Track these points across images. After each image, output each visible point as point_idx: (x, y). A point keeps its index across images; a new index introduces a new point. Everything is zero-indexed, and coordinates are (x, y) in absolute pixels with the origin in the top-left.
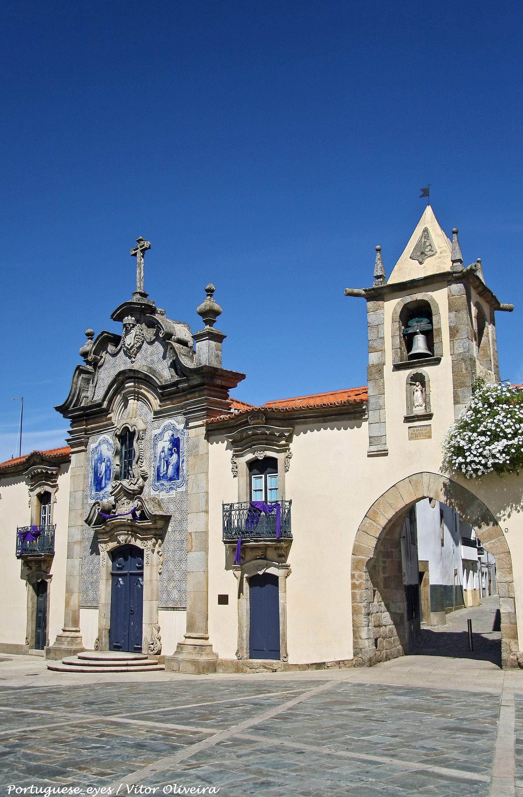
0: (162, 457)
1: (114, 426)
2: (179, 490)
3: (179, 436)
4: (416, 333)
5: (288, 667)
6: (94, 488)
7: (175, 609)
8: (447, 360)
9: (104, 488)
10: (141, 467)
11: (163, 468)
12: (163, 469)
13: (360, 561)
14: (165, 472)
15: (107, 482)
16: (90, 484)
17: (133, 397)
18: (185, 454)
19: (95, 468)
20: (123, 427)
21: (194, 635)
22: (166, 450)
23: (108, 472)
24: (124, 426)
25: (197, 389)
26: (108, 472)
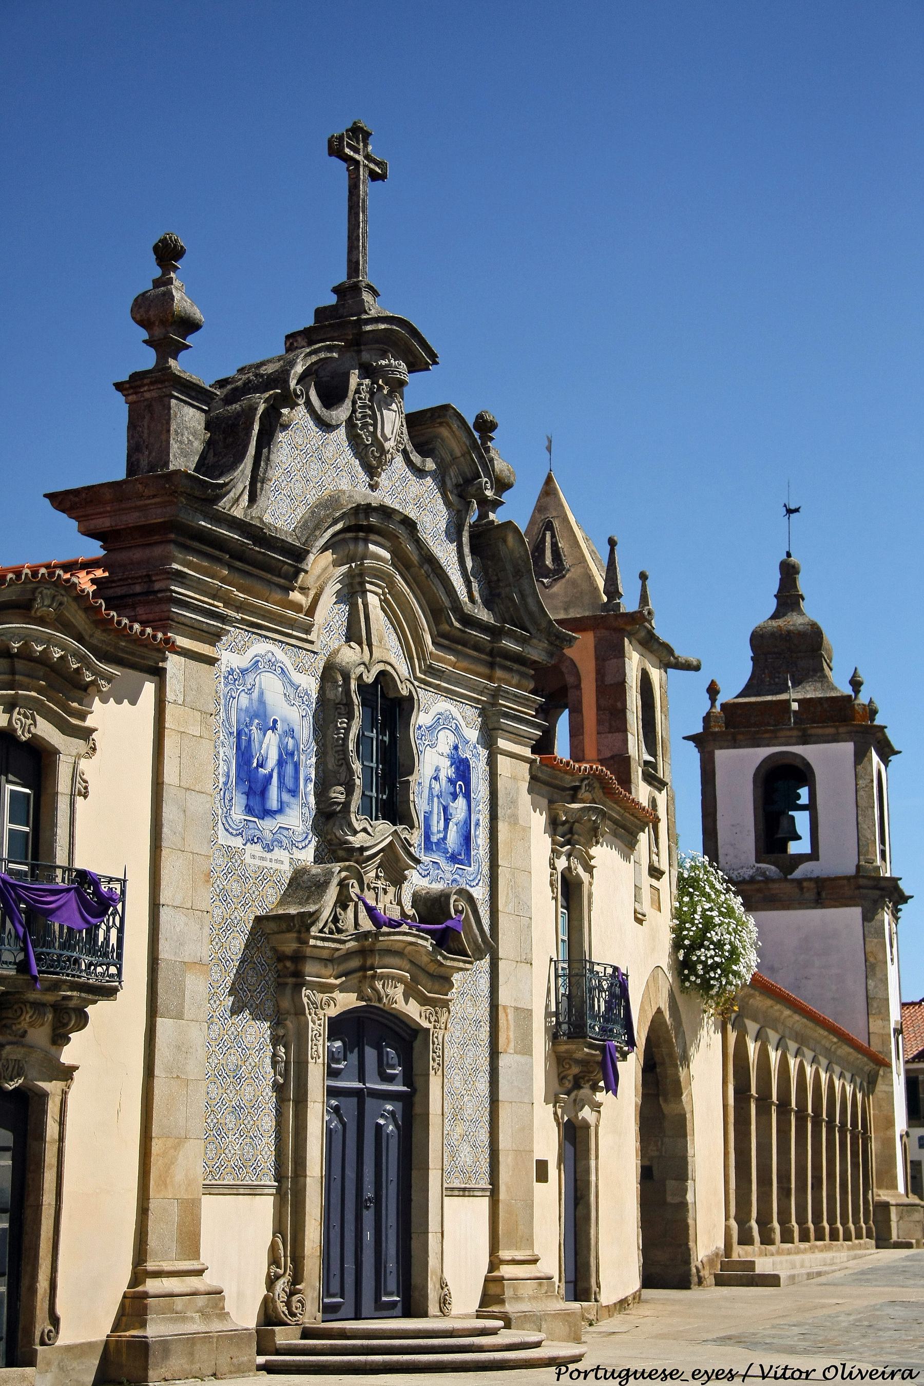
0: (435, 793)
1: (309, 638)
3: (468, 757)
6: (239, 801)
7: (467, 1193)
9: (276, 812)
11: (438, 822)
14: (442, 835)
15: (286, 797)
16: (222, 779)
17: (380, 591)
18: (481, 806)
23: (289, 769)
25: (516, 667)
26: (289, 769)
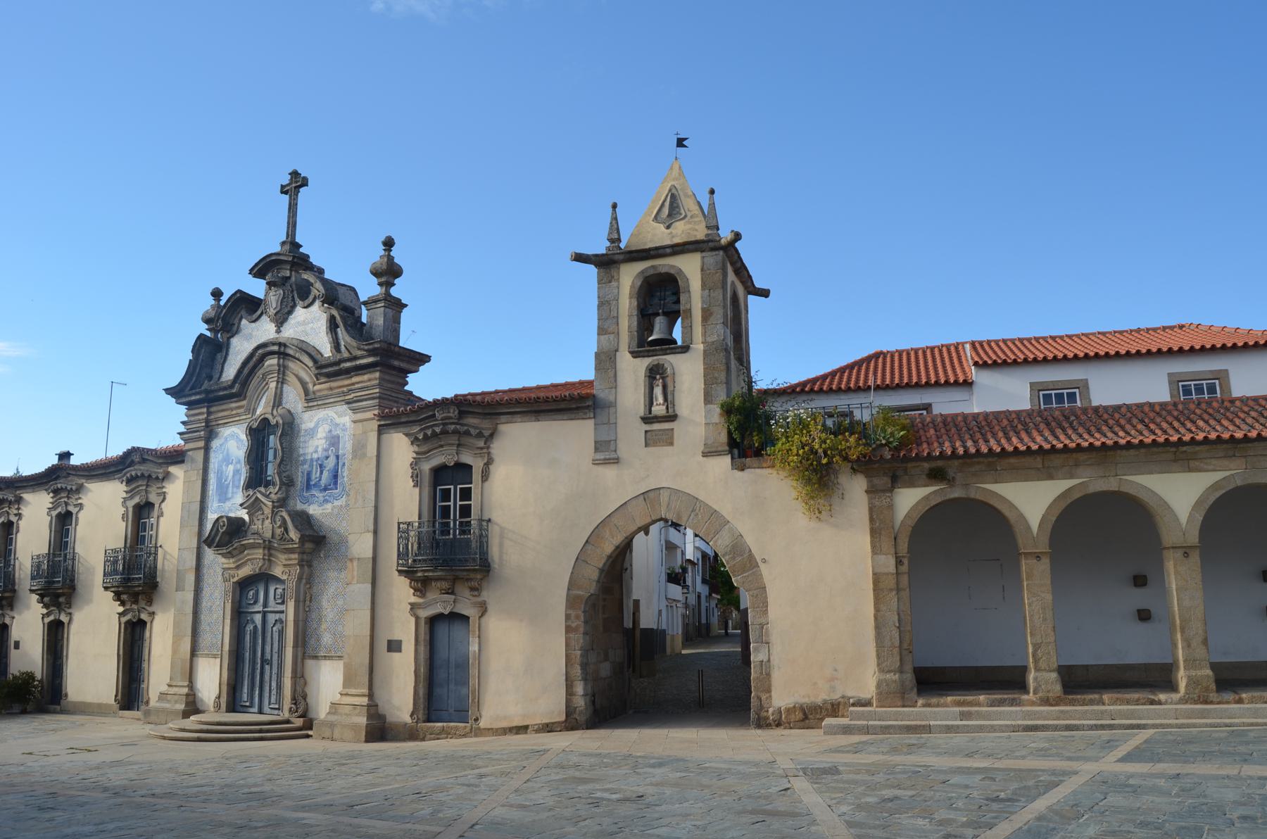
2: (337, 503)
4: (658, 314)
5: (479, 732)
8: (698, 347)
9: (230, 498)
10: (284, 472)
12: (315, 476)
13: (578, 597)
19: (218, 471)
20: (261, 418)
21: (353, 691)
22: (320, 449)
24: (262, 417)
